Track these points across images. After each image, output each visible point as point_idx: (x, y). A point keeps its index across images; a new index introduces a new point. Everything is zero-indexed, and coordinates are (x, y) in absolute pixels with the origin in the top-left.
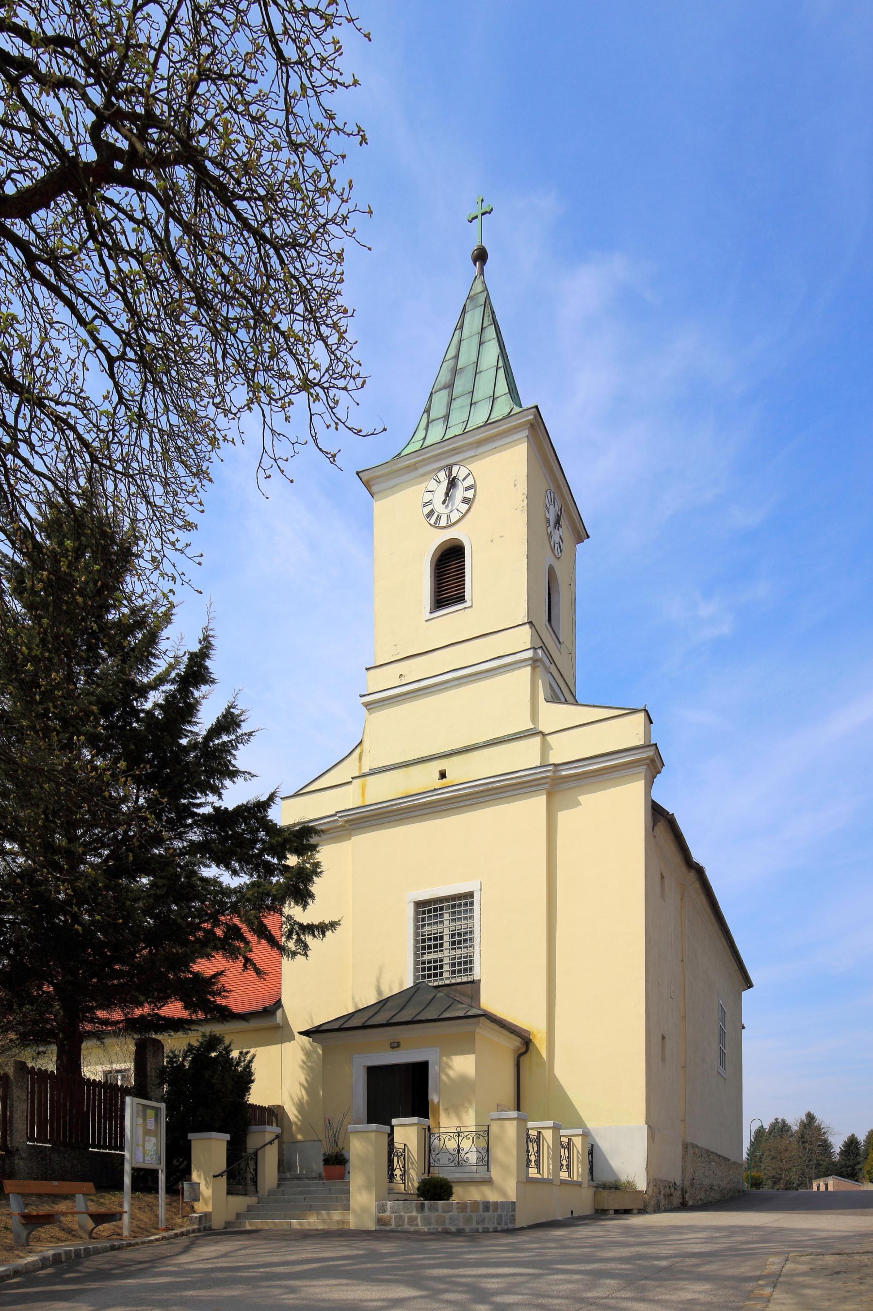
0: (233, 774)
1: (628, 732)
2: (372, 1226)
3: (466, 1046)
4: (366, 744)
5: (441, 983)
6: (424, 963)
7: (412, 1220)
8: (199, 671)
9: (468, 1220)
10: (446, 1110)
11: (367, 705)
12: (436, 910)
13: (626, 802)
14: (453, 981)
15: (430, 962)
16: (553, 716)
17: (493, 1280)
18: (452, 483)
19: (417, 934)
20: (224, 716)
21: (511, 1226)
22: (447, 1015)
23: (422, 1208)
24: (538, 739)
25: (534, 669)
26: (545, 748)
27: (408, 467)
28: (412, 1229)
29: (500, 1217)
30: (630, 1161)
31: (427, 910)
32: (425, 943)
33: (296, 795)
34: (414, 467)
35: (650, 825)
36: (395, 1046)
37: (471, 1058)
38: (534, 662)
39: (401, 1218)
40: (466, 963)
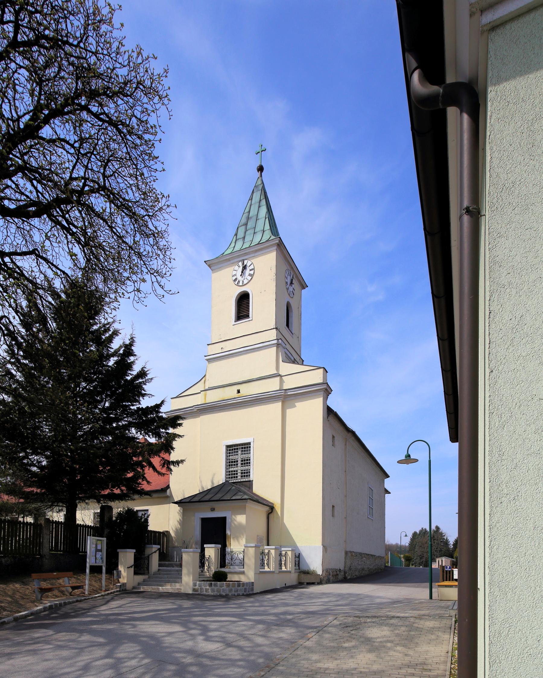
0: (144, 395)
1: (317, 377)
2: (191, 592)
3: (242, 511)
4: (207, 377)
5: (237, 481)
6: (229, 472)
7: (207, 590)
8: (129, 352)
9: (231, 591)
10: (233, 538)
11: (207, 360)
12: (235, 449)
13: (314, 407)
14: (242, 480)
15: (232, 472)
16: (286, 368)
17: (214, 624)
18: (245, 268)
19: (227, 459)
20: (140, 371)
21: (251, 592)
22: (234, 498)
23: (211, 585)
24: (278, 378)
25: (277, 348)
26: (282, 382)
27: (226, 260)
28: (207, 594)
29: (246, 589)
30: (315, 563)
31: (231, 449)
32: (230, 463)
33: (177, 397)
34: (229, 260)
35: (326, 416)
36: (213, 510)
37: (244, 516)
38: (278, 345)
39: (201, 589)
40: (247, 473)
